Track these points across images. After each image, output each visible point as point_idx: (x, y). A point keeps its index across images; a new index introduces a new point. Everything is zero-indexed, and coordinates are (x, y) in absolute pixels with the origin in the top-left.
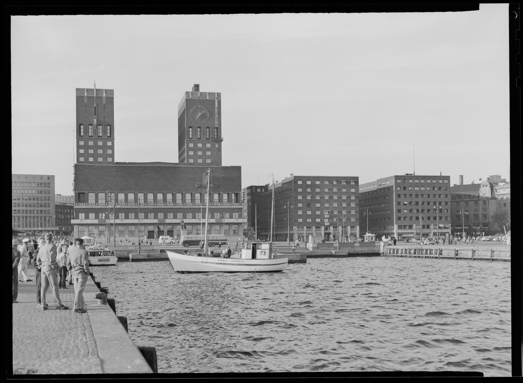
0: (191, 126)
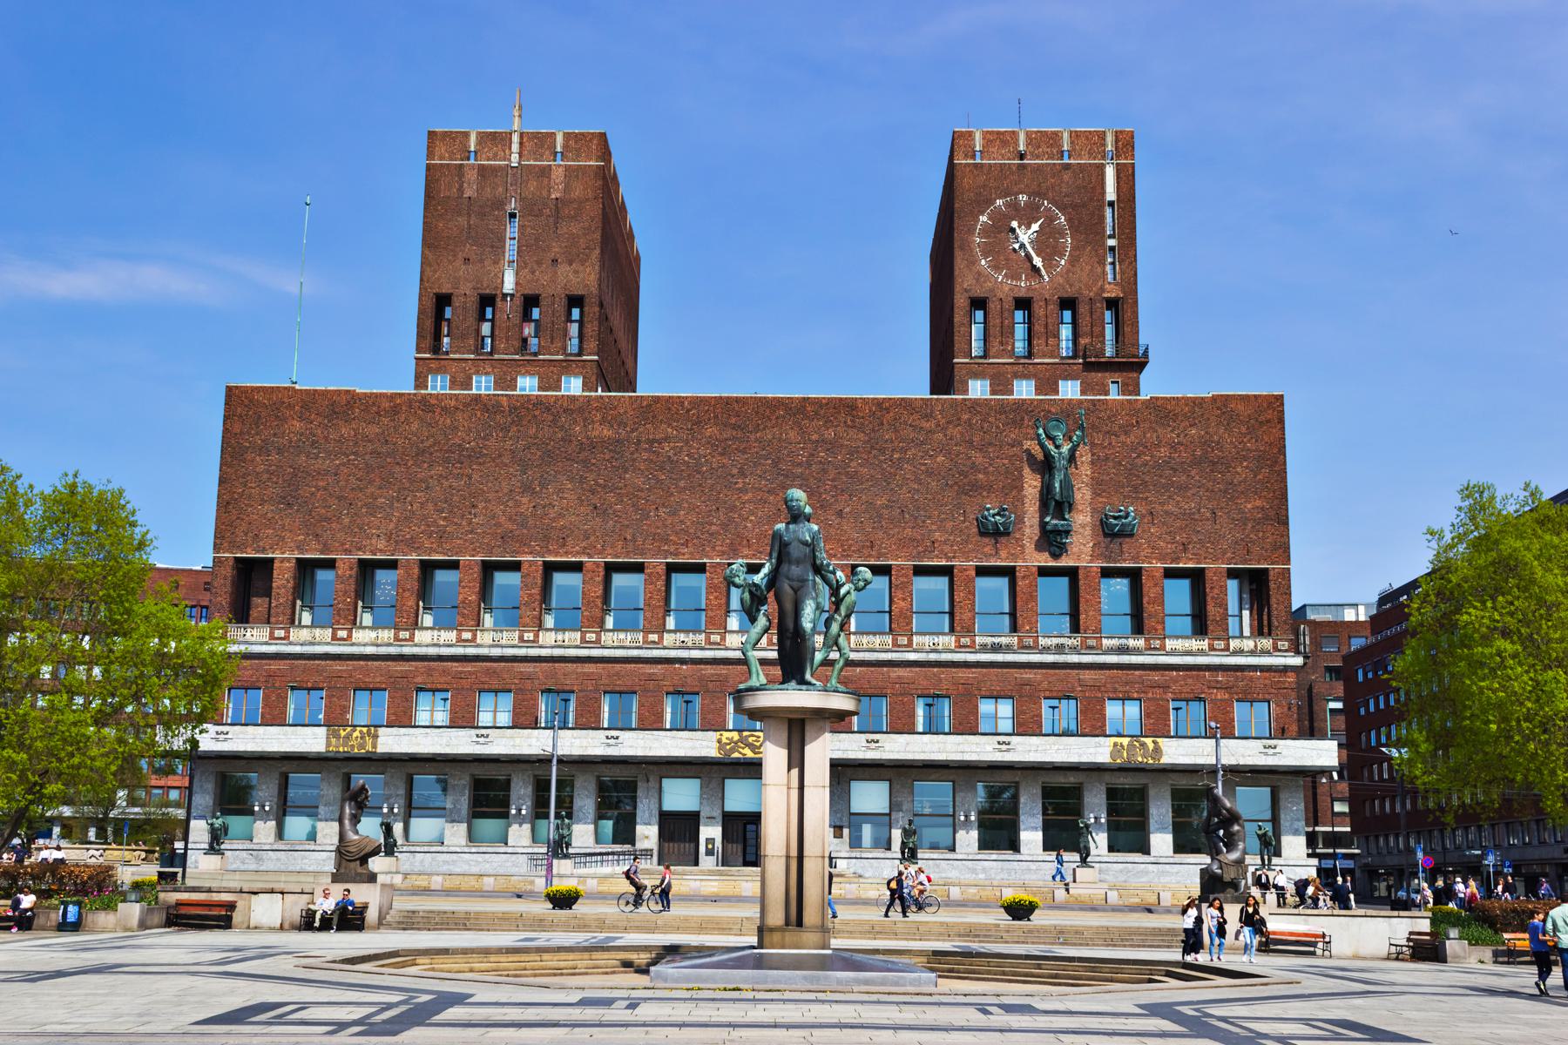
0: (978, 292)
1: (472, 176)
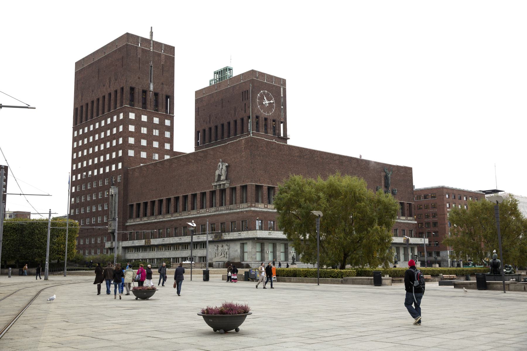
0: (258, 114)
1: (140, 51)
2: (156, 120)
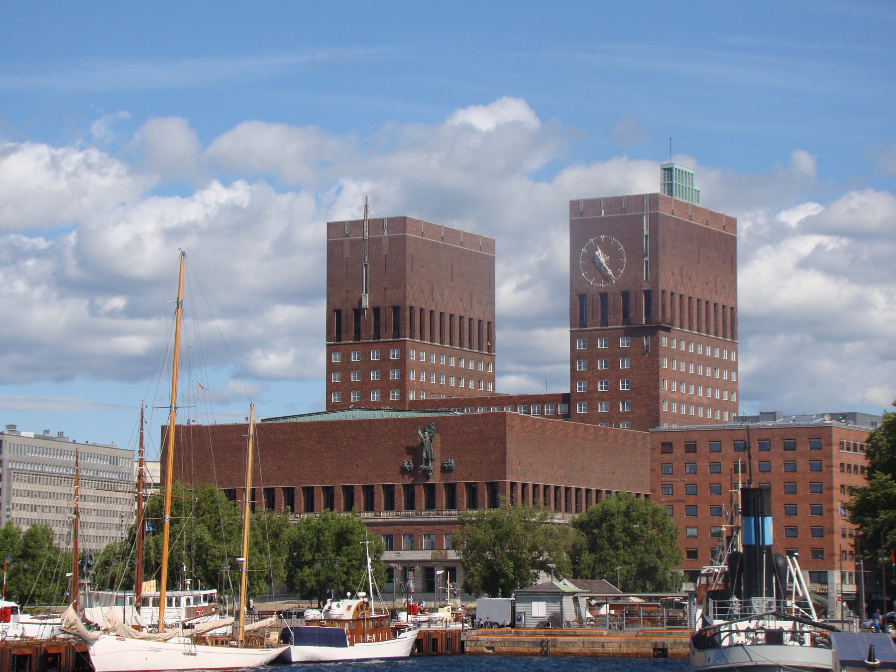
1: (347, 246)
2: (374, 356)
